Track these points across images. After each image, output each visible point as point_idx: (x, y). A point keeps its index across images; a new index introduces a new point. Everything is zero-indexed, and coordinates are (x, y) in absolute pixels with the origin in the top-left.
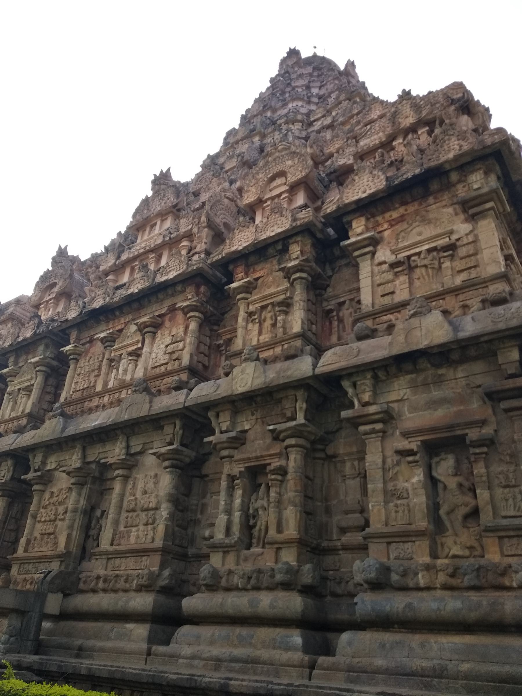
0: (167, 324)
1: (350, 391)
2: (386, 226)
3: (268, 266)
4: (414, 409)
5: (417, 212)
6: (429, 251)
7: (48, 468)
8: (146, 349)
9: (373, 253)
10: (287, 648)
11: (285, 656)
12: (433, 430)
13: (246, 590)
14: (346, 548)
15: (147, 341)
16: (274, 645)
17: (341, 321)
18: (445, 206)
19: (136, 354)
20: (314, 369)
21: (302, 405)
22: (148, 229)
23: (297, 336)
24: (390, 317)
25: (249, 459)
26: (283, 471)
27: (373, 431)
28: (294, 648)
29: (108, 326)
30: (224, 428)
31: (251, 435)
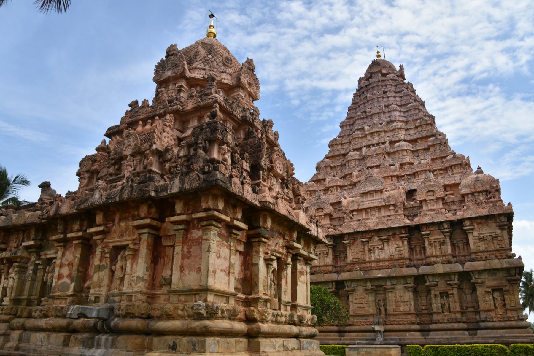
0: (392, 239)
1: (472, 275)
2: (475, 224)
3: (434, 227)
4: (489, 281)
5: (485, 223)
6: (489, 236)
7: (353, 286)
8: (386, 248)
9: (472, 233)
10: (464, 335)
11: (466, 336)
12: (495, 287)
13: (447, 323)
14: (469, 312)
15: (386, 245)
16: (460, 334)
17: (458, 247)
18: (493, 223)
19: (382, 249)
20: (463, 269)
21: (457, 277)
22: (369, 195)
23: (450, 255)
24: (480, 254)
25: (441, 290)
26: (452, 294)
27: (479, 286)
28: (466, 335)
29: (363, 235)
30: (431, 281)
31: (439, 283)
